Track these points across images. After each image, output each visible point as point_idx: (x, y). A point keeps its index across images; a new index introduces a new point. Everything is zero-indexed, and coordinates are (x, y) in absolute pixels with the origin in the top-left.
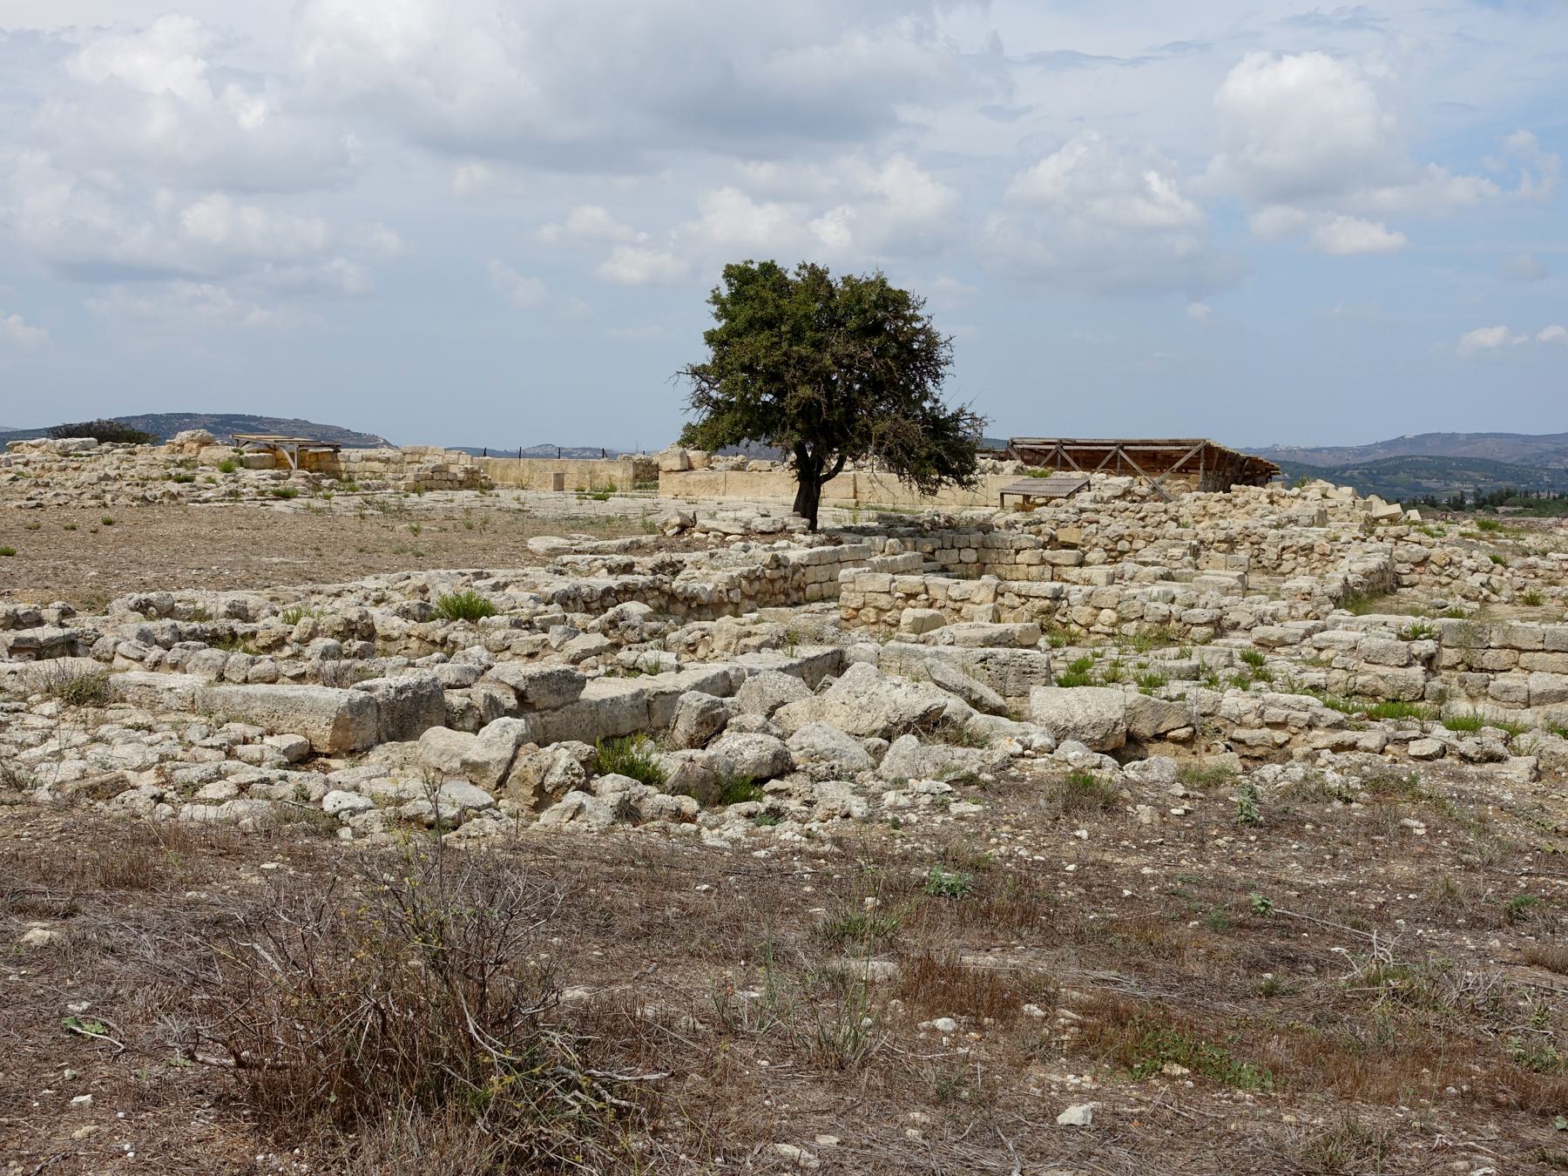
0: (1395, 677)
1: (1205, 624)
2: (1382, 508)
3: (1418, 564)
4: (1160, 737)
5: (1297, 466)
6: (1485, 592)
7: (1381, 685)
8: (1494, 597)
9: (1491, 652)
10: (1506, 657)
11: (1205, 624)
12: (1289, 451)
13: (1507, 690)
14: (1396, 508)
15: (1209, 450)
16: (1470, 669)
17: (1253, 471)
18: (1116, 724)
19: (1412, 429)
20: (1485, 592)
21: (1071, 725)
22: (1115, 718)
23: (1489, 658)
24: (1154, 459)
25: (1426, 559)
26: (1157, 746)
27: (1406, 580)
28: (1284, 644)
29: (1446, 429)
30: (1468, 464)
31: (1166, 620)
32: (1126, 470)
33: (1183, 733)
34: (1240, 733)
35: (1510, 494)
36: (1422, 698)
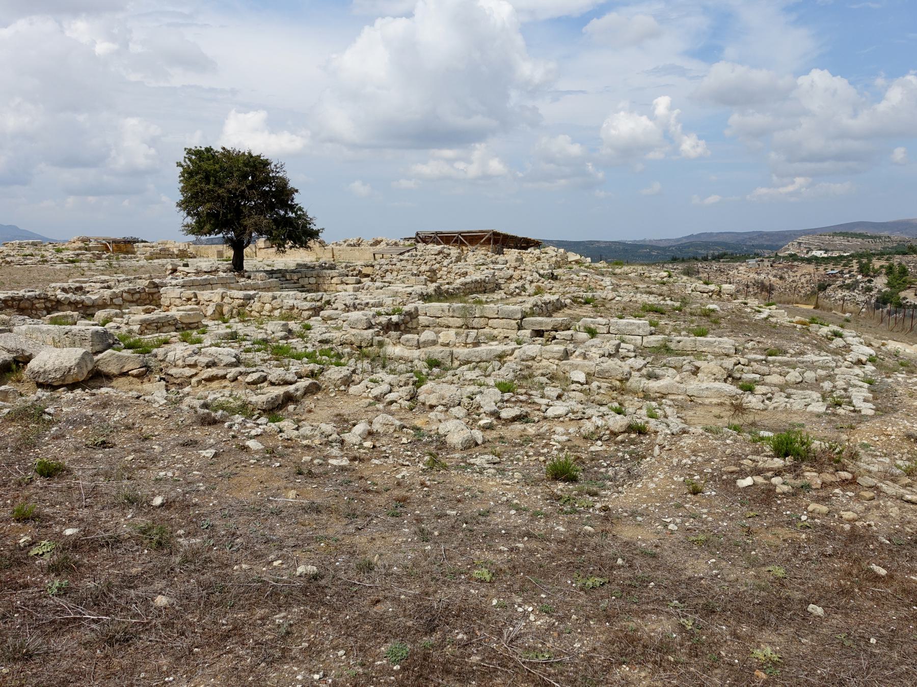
0: (360, 335)
1: (308, 310)
2: (573, 257)
3: (508, 279)
4: (125, 374)
5: (652, 246)
6: (517, 291)
7: (353, 339)
8: (523, 293)
9: (476, 320)
10: (483, 321)
11: (308, 310)
12: (650, 241)
13: (408, 341)
14: (578, 257)
15: (496, 234)
16: (468, 328)
17: (524, 244)
18: (70, 369)
19: (715, 230)
20: (517, 291)
21: (42, 370)
22: (68, 365)
23: (475, 322)
24: (472, 239)
25: (511, 277)
26: (122, 380)
27: (503, 286)
28: (332, 319)
29: (709, 231)
30: (717, 244)
31: (292, 308)
32: (438, 243)
33: (135, 372)
34: (172, 371)
35: (725, 254)
36: (372, 345)
